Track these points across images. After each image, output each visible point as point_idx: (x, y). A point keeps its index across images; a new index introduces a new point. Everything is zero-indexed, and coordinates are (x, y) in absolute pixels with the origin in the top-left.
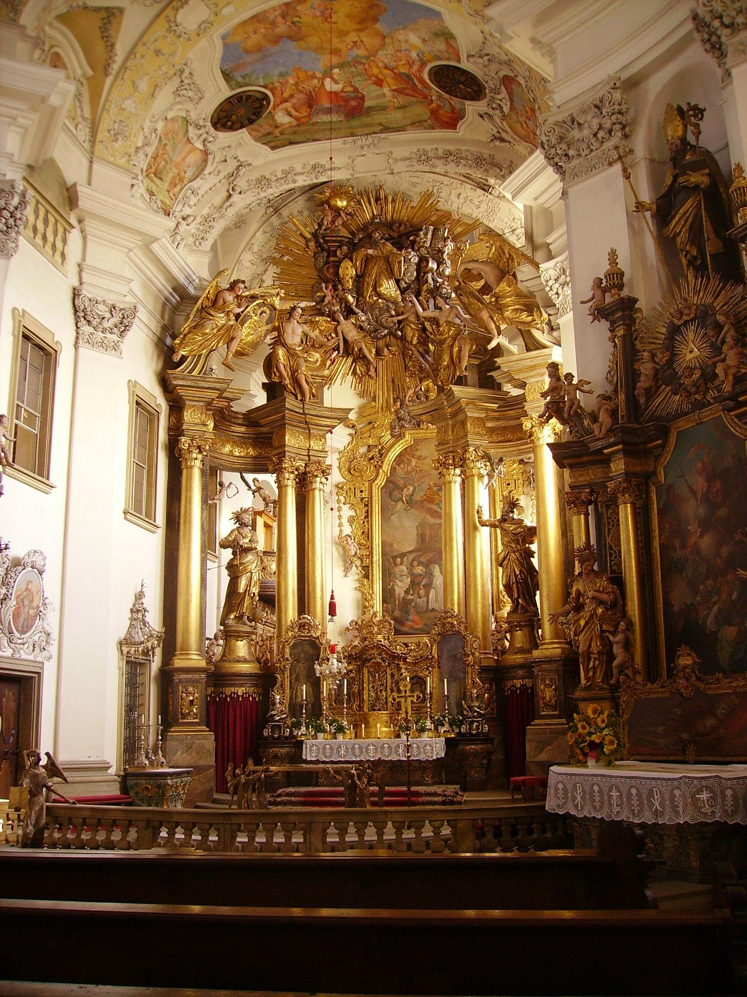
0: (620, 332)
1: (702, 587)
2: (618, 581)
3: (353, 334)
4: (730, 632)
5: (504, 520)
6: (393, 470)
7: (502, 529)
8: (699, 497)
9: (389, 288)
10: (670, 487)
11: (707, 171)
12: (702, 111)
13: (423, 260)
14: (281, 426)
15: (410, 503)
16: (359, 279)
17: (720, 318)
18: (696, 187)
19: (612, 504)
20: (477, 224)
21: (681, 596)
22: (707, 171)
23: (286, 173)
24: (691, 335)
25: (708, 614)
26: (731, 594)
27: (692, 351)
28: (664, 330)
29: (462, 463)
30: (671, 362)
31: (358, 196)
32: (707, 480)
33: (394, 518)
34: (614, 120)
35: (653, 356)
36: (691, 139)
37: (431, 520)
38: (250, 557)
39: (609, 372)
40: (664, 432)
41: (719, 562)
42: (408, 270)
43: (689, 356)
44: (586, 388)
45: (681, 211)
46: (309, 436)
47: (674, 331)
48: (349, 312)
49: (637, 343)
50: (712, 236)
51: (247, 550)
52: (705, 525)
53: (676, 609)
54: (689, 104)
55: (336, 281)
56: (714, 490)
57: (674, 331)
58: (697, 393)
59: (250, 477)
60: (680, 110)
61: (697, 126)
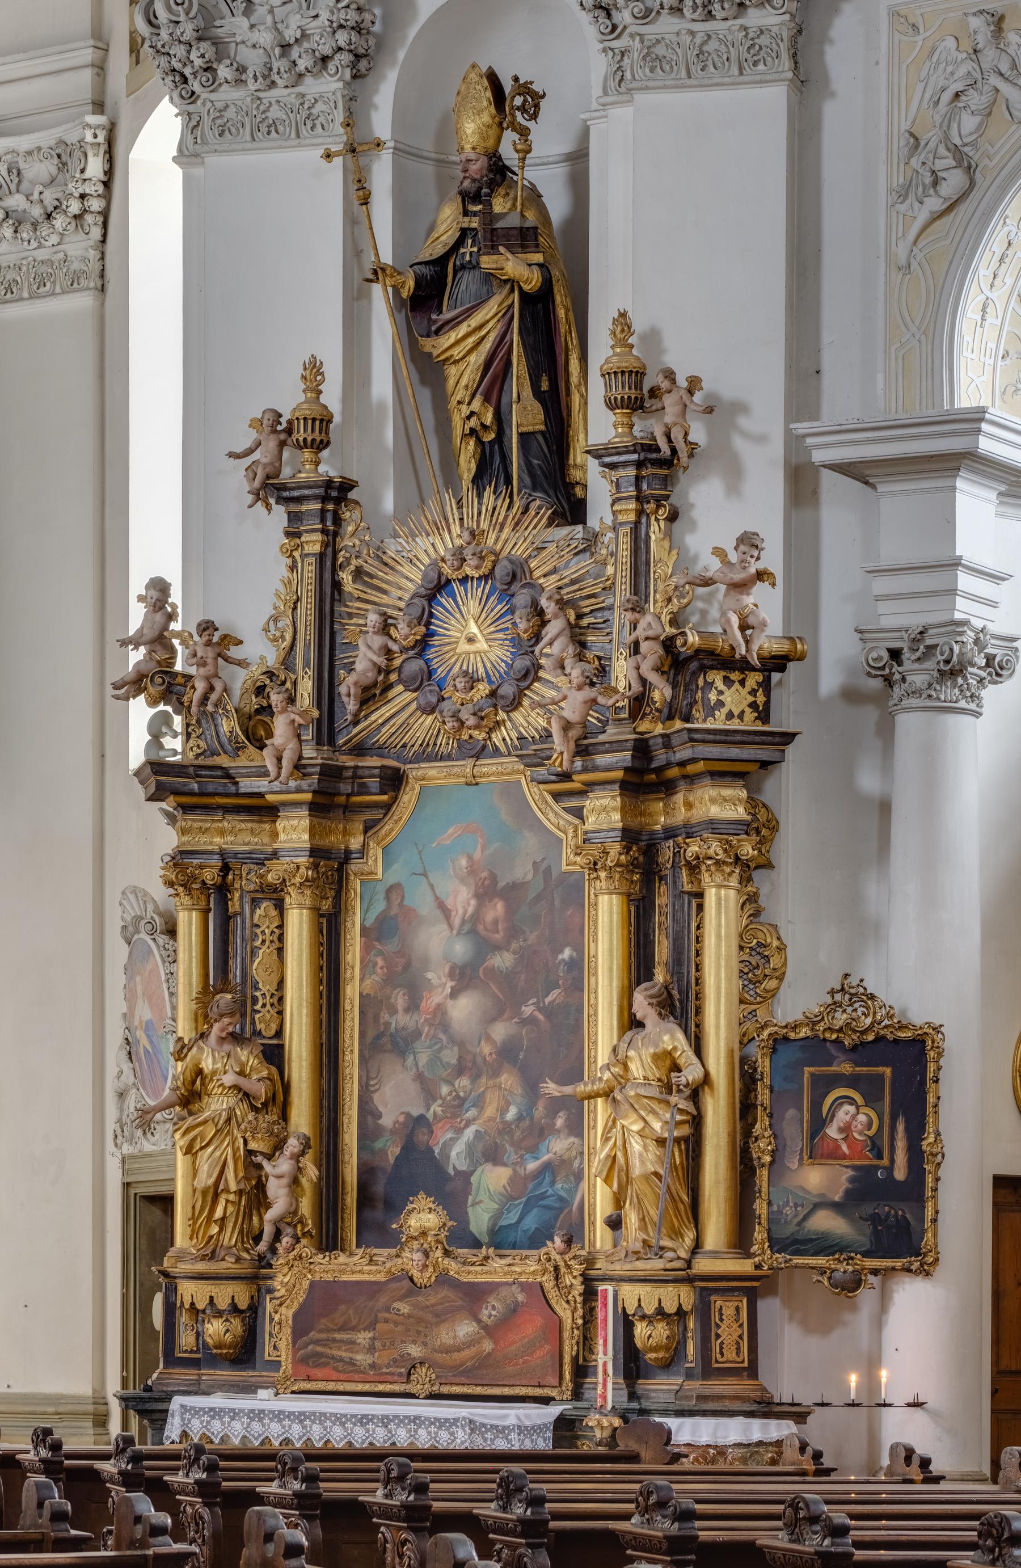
0: (313, 543)
1: (445, 1090)
2: (274, 1055)
4: (492, 1180)
8: (457, 922)
10: (393, 890)
11: (539, 258)
12: (538, 97)
17: (549, 607)
18: (512, 283)
21: (396, 1098)
22: (539, 258)
24: (473, 606)
25: (454, 1140)
26: (503, 1111)
27: (473, 637)
28: (417, 576)
30: (423, 645)
32: (477, 896)
34: (342, 43)
36: (508, 153)
39: (275, 619)
40: (394, 781)
41: (486, 1049)
43: (463, 647)
44: (234, 652)
45: (474, 322)
49: (346, 577)
50: (527, 391)
52: (464, 977)
53: (387, 1121)
54: (516, 79)
56: (489, 916)
57: (438, 587)
58: (477, 727)
60: (493, 80)
61: (524, 133)
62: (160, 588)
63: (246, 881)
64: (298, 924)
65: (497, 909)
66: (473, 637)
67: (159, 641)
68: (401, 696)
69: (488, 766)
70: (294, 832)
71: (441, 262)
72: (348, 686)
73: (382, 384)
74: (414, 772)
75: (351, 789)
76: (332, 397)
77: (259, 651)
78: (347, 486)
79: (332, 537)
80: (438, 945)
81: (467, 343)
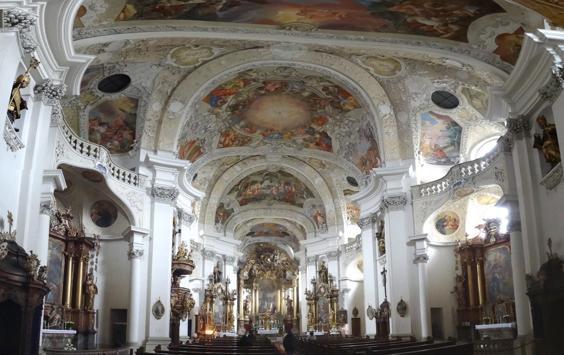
3: (263, 267)
9: (269, 260)
13: (274, 256)
14: (253, 282)
16: (264, 258)
20: (283, 250)
23: (254, 241)
29: (281, 289)
31: (264, 243)
42: (272, 257)
48: (262, 263)
55: (260, 258)
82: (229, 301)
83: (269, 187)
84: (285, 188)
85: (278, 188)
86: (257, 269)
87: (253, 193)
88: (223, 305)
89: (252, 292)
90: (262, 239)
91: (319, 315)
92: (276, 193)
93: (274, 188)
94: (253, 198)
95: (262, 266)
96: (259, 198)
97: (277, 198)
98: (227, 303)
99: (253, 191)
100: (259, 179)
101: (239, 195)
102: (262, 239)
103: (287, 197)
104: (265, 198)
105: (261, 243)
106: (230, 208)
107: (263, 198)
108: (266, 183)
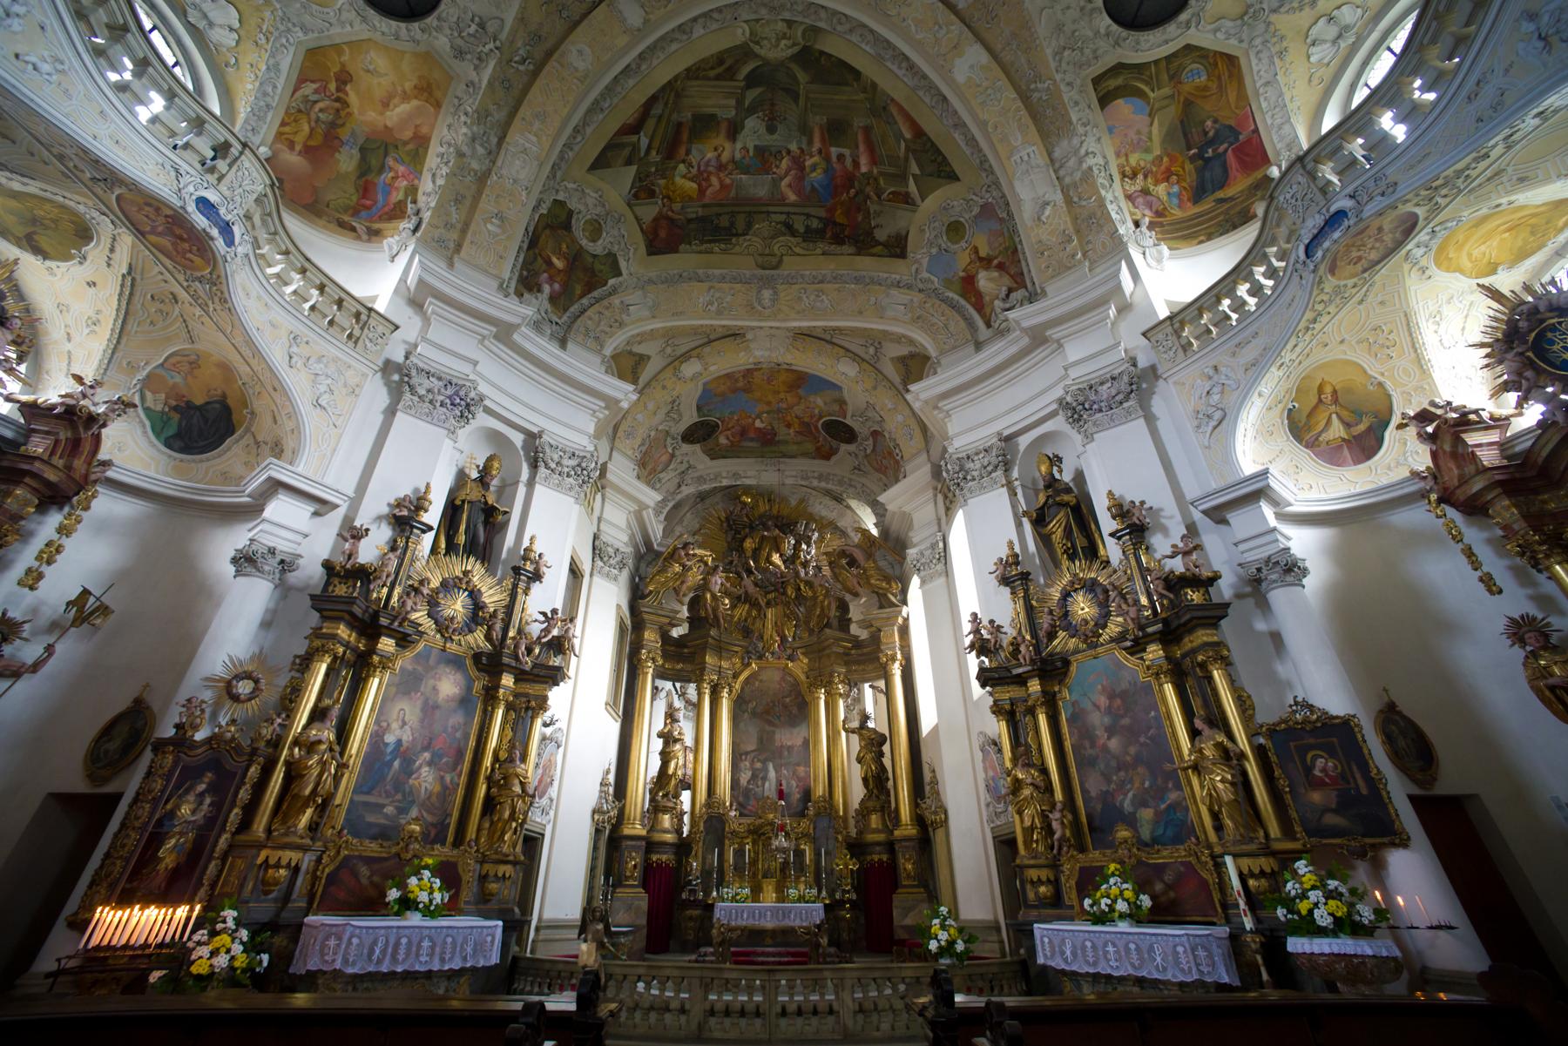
5: (863, 726)
6: (742, 689)
7: (861, 735)
14: (703, 649)
15: (754, 714)
19: (1031, 712)
24: (1080, 598)
27: (1083, 607)
29: (829, 685)
33: (742, 725)
35: (1051, 612)
37: (767, 728)
38: (678, 746)
40: (1067, 663)
46: (720, 658)
47: (1066, 595)
51: (676, 741)
59: (678, 685)
62: (975, 615)
63: (1020, 709)
64: (1042, 720)
65: (1118, 702)
66: (1083, 607)
67: (976, 631)
68: (1062, 634)
69: (1100, 650)
70: (1035, 686)
71: (1042, 508)
72: (1042, 634)
73: (1032, 547)
74: (1072, 659)
75: (1053, 669)
76: (1017, 549)
77: (1010, 632)
78: (1028, 574)
79: (1026, 591)
80: (1097, 720)
81: (1056, 527)
82: (508, 680)
83: (764, 158)
84: (827, 159)
85: (798, 164)
86: (726, 593)
87: (702, 191)
88: (464, 701)
89: (700, 694)
90: (751, 473)
91: (1095, 785)
92: (792, 197)
93: (785, 163)
94: (701, 220)
95: (747, 582)
96: (724, 222)
97: (800, 227)
98: (490, 695)
99: (701, 178)
100: (719, 102)
101: (642, 191)
102: (751, 473)
103: (839, 217)
104: (749, 225)
105: (747, 490)
106: (598, 248)
107: (740, 223)
108: (754, 132)
